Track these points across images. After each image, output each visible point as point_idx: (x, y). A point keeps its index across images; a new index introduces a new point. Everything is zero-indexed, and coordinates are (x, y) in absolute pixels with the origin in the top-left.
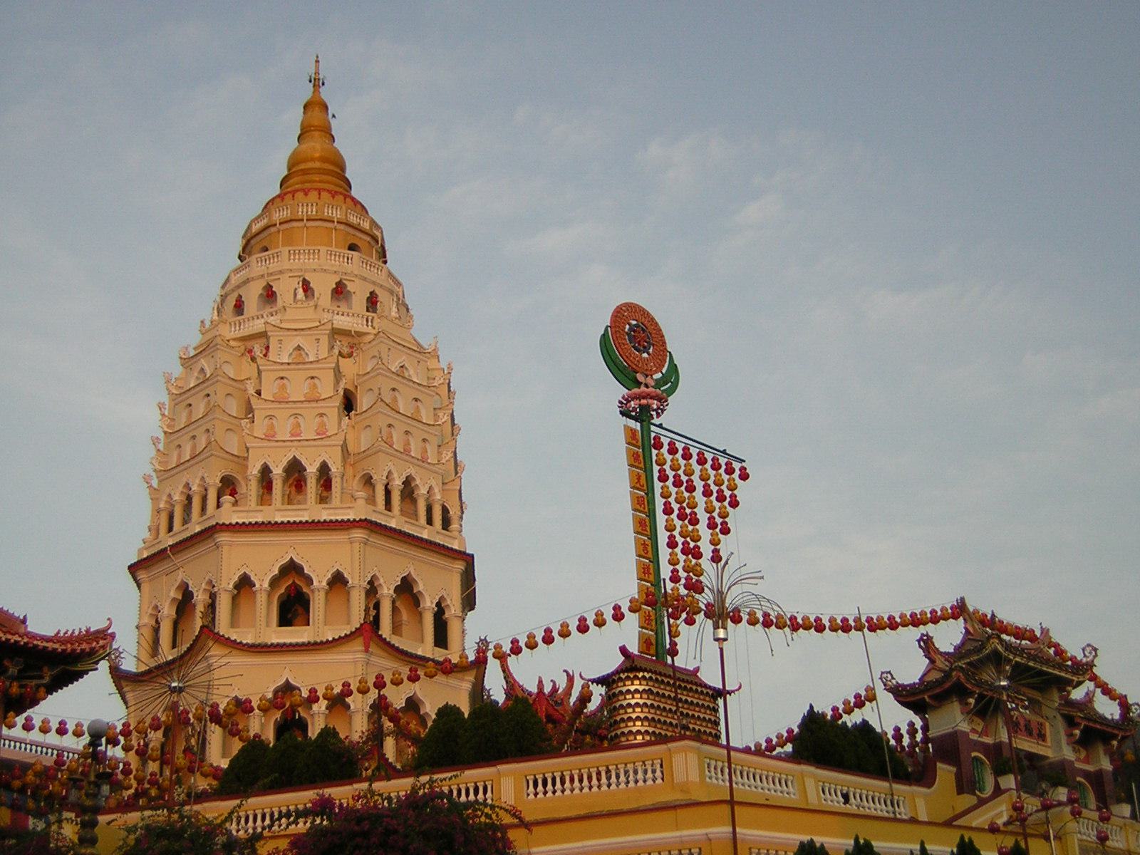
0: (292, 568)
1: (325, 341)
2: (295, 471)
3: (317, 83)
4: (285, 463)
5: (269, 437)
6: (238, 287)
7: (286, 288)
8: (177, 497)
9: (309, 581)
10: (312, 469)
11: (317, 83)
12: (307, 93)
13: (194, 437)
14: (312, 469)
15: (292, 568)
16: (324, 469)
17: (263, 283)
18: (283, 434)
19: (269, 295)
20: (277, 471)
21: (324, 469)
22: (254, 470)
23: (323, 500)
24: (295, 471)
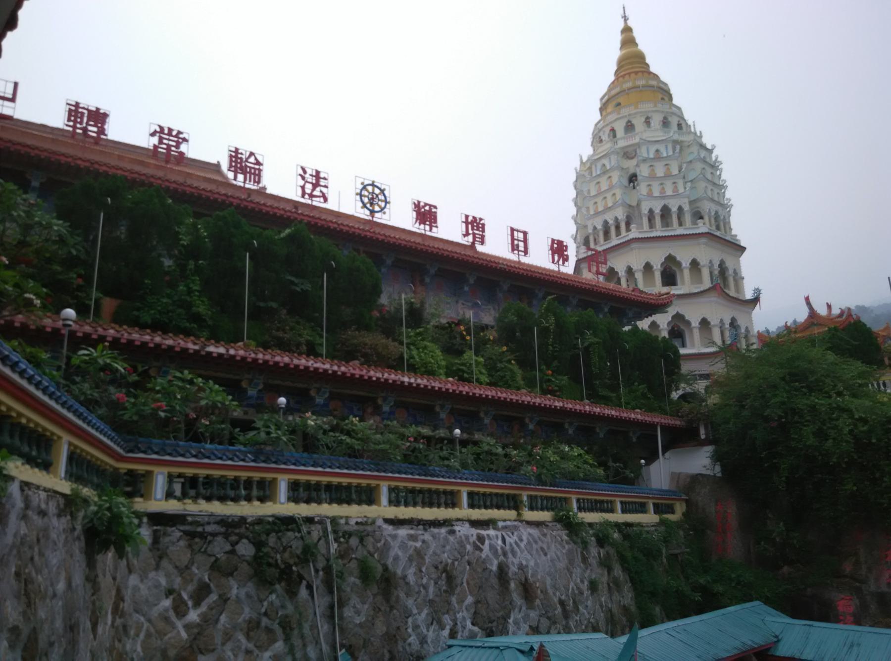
1: (670, 146)
2: (666, 212)
3: (625, 19)
4: (659, 208)
5: (650, 195)
6: (611, 123)
7: (638, 122)
10: (674, 209)
11: (625, 19)
12: (621, 25)
14: (674, 209)
16: (680, 209)
17: (626, 120)
18: (656, 193)
20: (657, 211)
21: (680, 209)
22: (645, 210)
23: (680, 224)
24: (666, 212)
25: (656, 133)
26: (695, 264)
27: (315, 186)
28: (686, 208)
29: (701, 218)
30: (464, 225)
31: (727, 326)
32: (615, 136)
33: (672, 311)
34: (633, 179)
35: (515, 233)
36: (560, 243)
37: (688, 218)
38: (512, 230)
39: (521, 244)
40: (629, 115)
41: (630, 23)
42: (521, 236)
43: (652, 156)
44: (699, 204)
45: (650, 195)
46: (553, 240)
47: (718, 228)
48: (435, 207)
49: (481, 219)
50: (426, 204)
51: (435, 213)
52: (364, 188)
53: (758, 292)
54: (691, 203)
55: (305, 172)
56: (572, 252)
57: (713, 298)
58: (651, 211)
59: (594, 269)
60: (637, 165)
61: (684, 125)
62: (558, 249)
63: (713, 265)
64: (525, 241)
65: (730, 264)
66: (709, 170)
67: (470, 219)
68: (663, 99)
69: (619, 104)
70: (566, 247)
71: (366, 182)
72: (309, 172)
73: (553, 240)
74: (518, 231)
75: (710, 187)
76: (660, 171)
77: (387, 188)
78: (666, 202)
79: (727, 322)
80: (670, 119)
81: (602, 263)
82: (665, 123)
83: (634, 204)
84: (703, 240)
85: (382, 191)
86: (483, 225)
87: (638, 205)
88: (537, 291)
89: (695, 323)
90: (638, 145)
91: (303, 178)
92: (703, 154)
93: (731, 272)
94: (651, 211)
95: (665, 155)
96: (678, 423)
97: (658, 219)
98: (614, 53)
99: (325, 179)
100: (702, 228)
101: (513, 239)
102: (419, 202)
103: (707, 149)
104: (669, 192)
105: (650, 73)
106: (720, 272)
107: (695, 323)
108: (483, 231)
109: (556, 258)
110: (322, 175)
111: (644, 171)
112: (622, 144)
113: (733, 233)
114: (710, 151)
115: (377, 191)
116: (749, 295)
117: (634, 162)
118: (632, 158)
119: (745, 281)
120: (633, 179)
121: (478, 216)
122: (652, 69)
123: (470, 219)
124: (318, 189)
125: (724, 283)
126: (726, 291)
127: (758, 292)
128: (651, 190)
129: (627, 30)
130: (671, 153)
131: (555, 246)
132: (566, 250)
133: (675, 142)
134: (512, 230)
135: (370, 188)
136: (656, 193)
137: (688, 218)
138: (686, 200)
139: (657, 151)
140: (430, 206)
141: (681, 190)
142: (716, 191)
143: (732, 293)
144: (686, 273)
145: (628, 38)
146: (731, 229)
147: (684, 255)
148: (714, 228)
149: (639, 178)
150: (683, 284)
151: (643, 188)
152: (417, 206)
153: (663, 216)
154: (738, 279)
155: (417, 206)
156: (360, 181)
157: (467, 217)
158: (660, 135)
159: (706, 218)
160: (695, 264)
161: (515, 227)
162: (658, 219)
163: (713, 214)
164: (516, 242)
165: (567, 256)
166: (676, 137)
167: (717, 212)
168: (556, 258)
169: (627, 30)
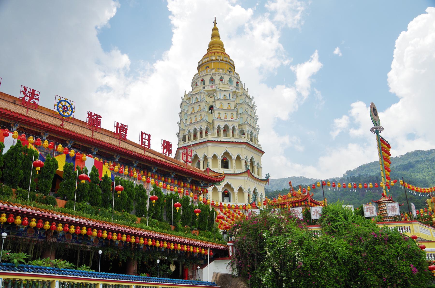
0: (226, 153)
3: (215, 23)
5: (219, 118)
7: (217, 79)
8: (192, 131)
9: (231, 157)
10: (231, 128)
11: (215, 23)
12: (213, 26)
13: (196, 116)
14: (231, 128)
15: (226, 153)
17: (210, 76)
18: (223, 118)
19: (212, 80)
20: (222, 127)
21: (234, 128)
23: (233, 136)
25: (225, 86)
26: (238, 158)
27: (31, 98)
28: (237, 127)
29: (244, 134)
30: (116, 128)
31: (252, 193)
32: (204, 84)
33: (223, 184)
34: (211, 108)
35: (144, 135)
36: (168, 143)
37: (237, 133)
38: (143, 133)
39: (147, 142)
40: (212, 74)
41: (217, 26)
42: (147, 137)
43: (222, 98)
44: (243, 127)
45: (219, 118)
46: (164, 141)
47: (251, 140)
48: (100, 117)
49: (126, 126)
50: (95, 115)
51: (100, 120)
52: (60, 102)
53: (268, 175)
54: (239, 125)
55: (26, 90)
56: (174, 149)
57: (246, 176)
58: (219, 127)
59: (185, 159)
60: (214, 101)
61: (239, 84)
62: (167, 146)
63: (247, 159)
64: (149, 140)
65: (256, 160)
66: (250, 109)
67: (120, 125)
68: (230, 68)
69: (208, 67)
70: (171, 145)
71: (62, 99)
72: (28, 90)
73: (164, 141)
74: (146, 134)
75: (249, 118)
76: (225, 107)
77: (74, 103)
78: (227, 123)
79: (252, 190)
80: (233, 80)
81: (189, 156)
82: (230, 81)
83: (211, 122)
84: (244, 146)
85: (71, 105)
86: (127, 129)
87: (213, 122)
88: (153, 168)
89: (236, 190)
90: (216, 91)
91: (24, 93)
92: (247, 100)
93: (256, 164)
94: (219, 127)
95: (228, 98)
96: (222, 247)
97: (222, 132)
98: (208, 40)
99: (37, 95)
100: (243, 139)
101: (142, 138)
102: (91, 113)
103: (249, 98)
104: (229, 118)
105: (225, 54)
106: (250, 163)
107: (236, 190)
108: (126, 132)
109: (165, 151)
110: (36, 93)
111: (217, 105)
112: (207, 88)
113: (259, 143)
114: (251, 100)
115: (67, 105)
116: (264, 177)
117: (213, 99)
118: (212, 97)
119: (263, 169)
120: (211, 108)
121: (124, 124)
122: (226, 52)
123: (120, 125)
124: (33, 100)
125: (251, 170)
126: (253, 174)
127: (268, 175)
128: (220, 116)
129: (215, 29)
130: (231, 98)
131: (165, 144)
132: (171, 147)
133: (234, 92)
134: (143, 133)
135: (63, 103)
136: (223, 118)
137: (237, 133)
138: (237, 124)
139: (225, 95)
140: (98, 115)
141: (235, 118)
142: (252, 120)
143: (256, 175)
144: (234, 162)
145: (215, 34)
146: (258, 141)
147: (234, 152)
148: (250, 140)
149: (214, 108)
150: (232, 168)
151: (216, 114)
152: (90, 115)
153: (224, 130)
154: (259, 167)
155: (90, 115)
156: (58, 98)
157: (118, 124)
158: (227, 87)
159: (246, 134)
160: (238, 158)
161: (144, 132)
162: (222, 132)
163: (250, 132)
164: (144, 140)
165: (171, 150)
166: (235, 90)
167: (251, 132)
168: (165, 151)
169: (215, 29)
